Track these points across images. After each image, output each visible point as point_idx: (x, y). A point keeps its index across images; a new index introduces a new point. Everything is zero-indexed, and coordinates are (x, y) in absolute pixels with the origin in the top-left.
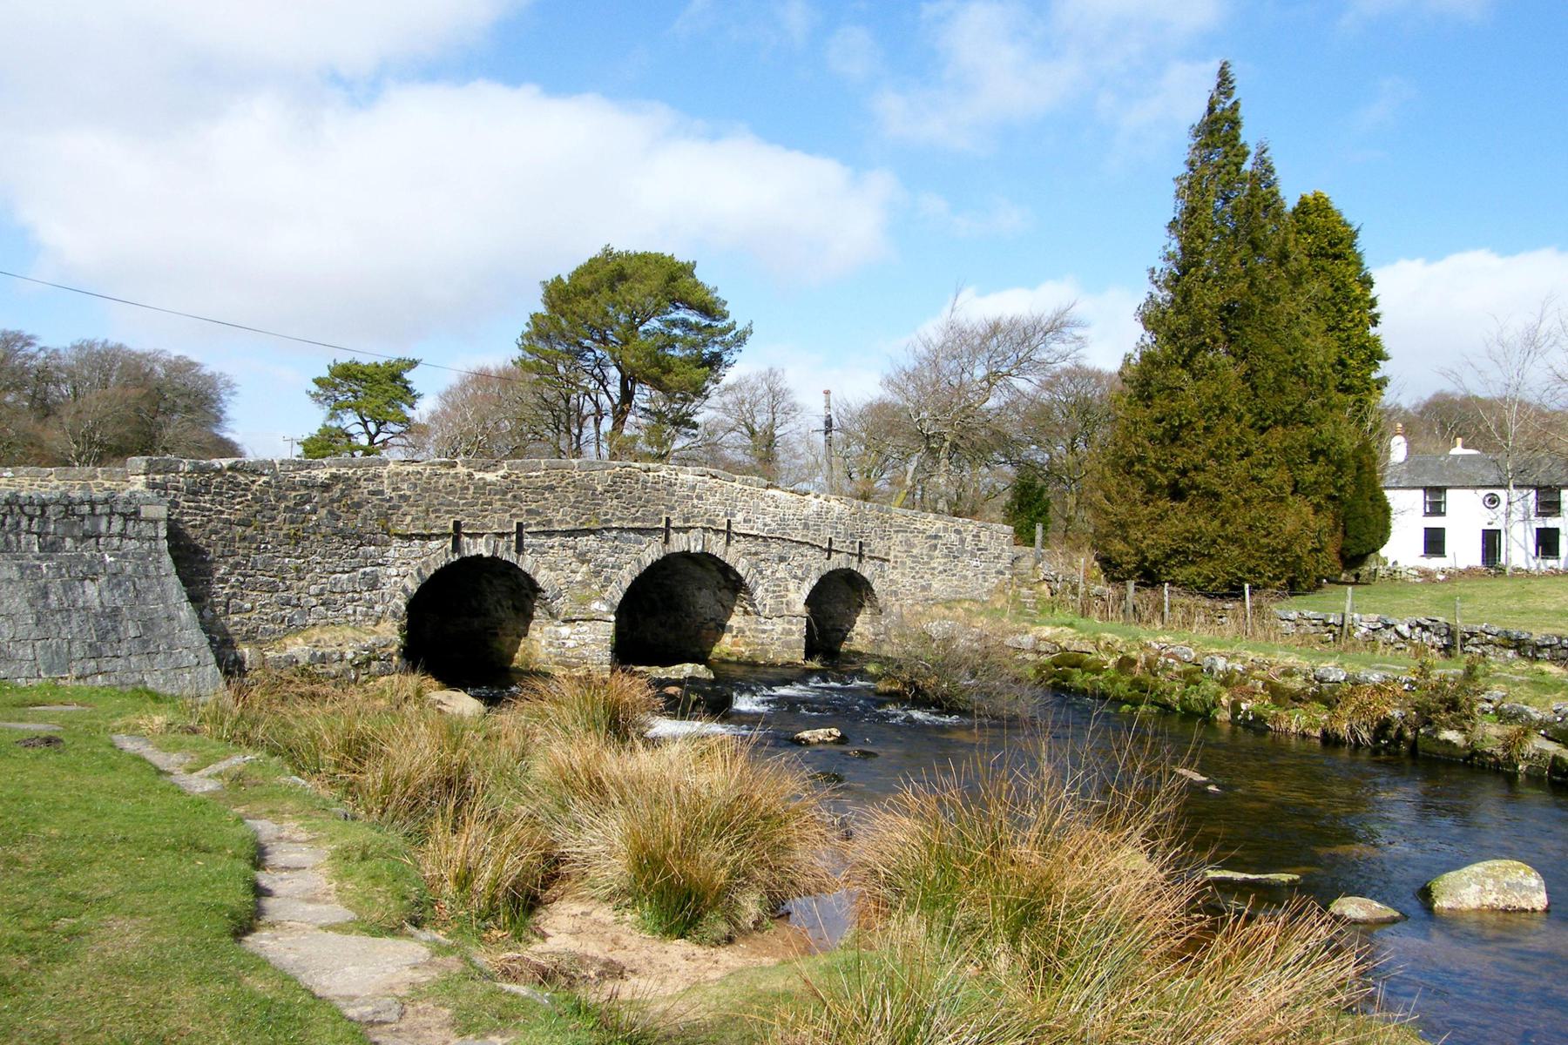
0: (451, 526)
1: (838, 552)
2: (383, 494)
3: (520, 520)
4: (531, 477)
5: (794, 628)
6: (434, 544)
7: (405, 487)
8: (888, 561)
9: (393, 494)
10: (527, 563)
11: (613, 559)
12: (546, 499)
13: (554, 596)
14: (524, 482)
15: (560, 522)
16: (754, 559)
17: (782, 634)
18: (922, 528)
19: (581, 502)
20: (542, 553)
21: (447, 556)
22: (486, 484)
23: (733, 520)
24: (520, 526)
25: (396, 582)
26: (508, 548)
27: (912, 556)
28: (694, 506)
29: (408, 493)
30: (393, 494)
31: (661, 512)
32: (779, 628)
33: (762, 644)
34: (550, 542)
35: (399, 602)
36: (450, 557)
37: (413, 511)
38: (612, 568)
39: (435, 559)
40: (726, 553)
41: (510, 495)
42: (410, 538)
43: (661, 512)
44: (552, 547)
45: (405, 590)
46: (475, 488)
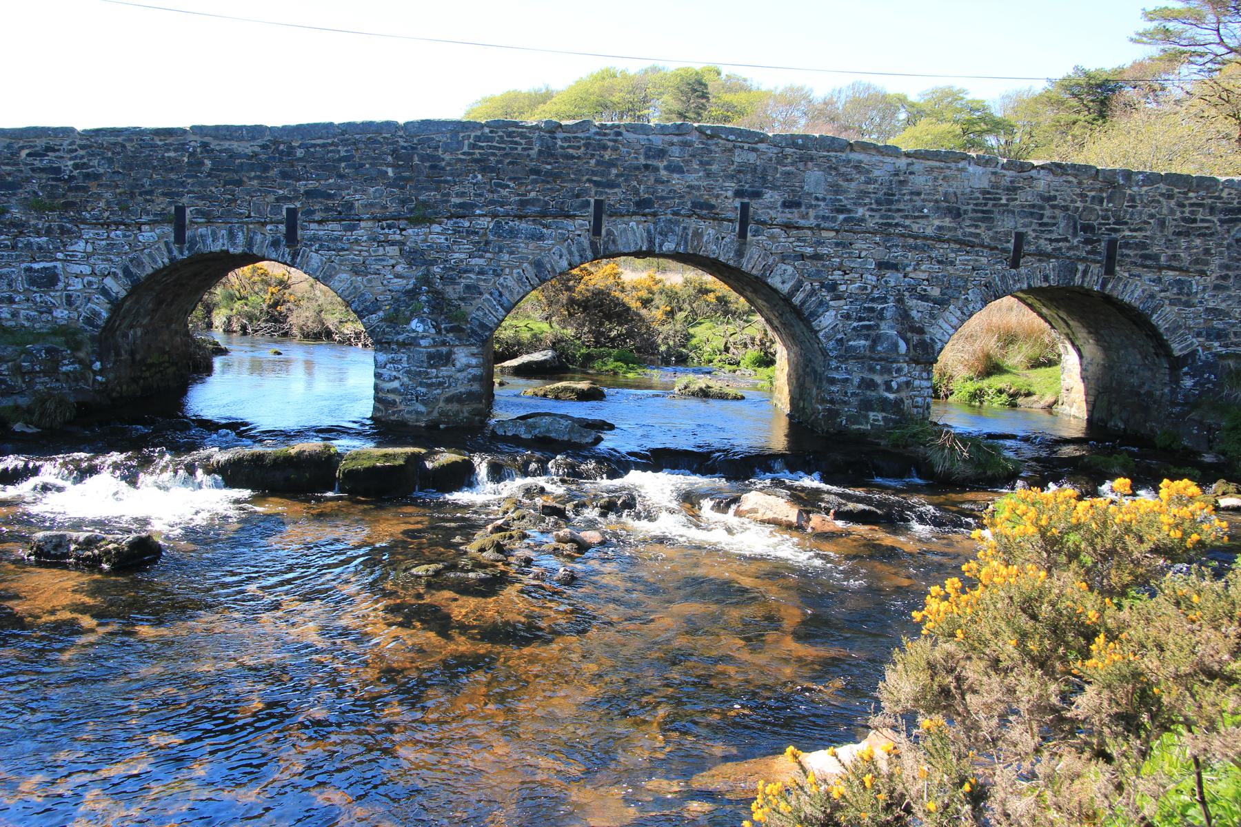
1: (1042, 255)
5: (878, 379)
7: (95, 162)
8: (1202, 273)
9: (76, 173)
11: (481, 261)
16: (810, 266)
17: (859, 387)
21: (170, 251)
22: (233, 155)
23: (754, 205)
24: (292, 213)
28: (659, 181)
30: (76, 173)
31: (585, 192)
32: (856, 381)
33: (832, 401)
35: (97, 308)
36: (176, 253)
37: (108, 195)
38: (481, 272)
39: (150, 255)
40: (740, 254)
41: (273, 173)
42: (107, 225)
43: (585, 192)
45: (105, 292)
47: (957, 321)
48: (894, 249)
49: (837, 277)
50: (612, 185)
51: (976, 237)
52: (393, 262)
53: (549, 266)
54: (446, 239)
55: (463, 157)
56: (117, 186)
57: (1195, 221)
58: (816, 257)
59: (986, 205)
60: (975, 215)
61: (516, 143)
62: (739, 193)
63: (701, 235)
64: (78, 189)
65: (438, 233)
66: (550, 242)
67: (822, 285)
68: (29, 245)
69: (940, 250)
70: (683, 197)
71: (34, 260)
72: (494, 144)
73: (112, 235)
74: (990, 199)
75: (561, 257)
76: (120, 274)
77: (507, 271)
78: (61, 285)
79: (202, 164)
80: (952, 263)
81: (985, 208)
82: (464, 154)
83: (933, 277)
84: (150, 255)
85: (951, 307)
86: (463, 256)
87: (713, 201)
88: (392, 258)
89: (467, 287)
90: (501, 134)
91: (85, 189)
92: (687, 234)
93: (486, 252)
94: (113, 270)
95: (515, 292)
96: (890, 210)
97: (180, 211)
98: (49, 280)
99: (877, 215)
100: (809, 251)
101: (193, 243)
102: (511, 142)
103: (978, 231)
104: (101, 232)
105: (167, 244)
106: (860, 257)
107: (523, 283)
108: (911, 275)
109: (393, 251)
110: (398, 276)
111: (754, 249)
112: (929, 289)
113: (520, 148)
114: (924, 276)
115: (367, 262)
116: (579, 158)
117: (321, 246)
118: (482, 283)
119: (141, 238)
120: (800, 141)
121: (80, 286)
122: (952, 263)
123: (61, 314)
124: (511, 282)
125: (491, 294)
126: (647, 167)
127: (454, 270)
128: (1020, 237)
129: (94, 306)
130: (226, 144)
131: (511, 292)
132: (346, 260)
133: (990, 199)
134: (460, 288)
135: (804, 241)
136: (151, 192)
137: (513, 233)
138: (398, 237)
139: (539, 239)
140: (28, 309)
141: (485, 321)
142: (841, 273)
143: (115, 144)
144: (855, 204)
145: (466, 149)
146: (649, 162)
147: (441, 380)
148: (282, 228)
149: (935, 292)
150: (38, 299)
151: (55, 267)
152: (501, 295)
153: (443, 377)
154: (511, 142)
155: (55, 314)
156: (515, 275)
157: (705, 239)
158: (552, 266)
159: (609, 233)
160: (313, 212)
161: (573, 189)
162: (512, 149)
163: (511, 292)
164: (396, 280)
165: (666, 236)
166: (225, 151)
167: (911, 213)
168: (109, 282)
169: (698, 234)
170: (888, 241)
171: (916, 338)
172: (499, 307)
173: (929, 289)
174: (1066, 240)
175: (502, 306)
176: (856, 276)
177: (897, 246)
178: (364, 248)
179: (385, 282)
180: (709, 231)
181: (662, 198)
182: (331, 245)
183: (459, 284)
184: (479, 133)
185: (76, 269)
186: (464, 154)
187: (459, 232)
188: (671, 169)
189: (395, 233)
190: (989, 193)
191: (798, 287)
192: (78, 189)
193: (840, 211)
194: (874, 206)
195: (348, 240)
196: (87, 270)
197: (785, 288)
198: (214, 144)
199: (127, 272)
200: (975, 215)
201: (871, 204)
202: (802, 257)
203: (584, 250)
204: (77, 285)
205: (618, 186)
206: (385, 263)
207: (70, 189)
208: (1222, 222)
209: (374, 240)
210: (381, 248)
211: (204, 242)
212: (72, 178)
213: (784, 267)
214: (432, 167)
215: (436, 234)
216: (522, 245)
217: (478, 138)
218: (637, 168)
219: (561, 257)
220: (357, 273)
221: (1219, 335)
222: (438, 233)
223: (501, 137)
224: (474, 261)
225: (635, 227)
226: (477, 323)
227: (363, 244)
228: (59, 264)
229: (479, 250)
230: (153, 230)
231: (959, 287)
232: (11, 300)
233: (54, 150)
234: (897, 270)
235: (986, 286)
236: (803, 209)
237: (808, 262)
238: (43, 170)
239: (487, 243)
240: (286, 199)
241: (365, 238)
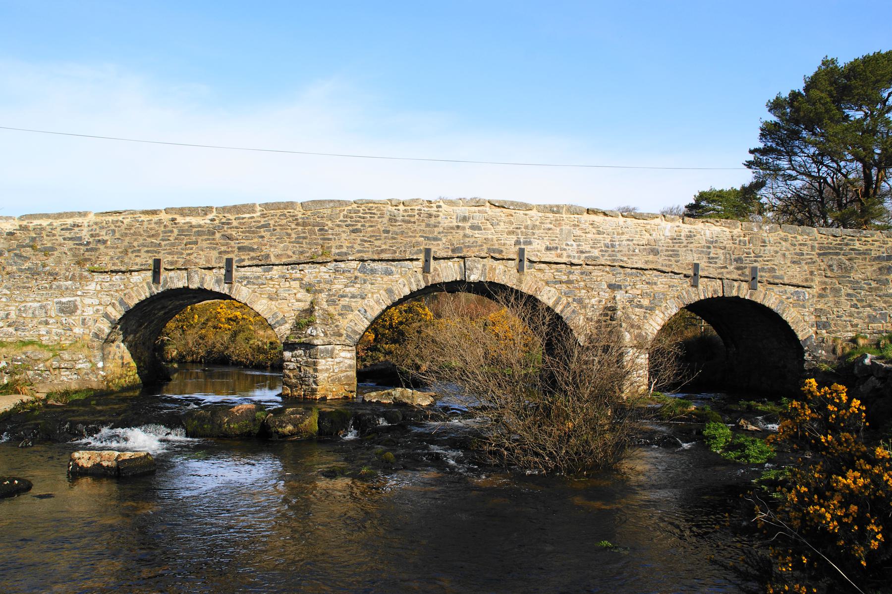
0: (151, 262)
2: (81, 240)
3: (229, 256)
4: (243, 218)
6: (136, 278)
10: (242, 293)
12: (263, 237)
13: (277, 322)
14: (235, 223)
15: (278, 256)
18: (863, 248)
19: (304, 238)
20: (259, 285)
21: (150, 288)
23: (527, 248)
25: (98, 310)
26: (218, 281)
27: (850, 282)
28: (465, 236)
29: (105, 238)
30: (91, 240)
34: (269, 275)
35: (102, 327)
36: (154, 289)
38: (353, 297)
44: (271, 279)
45: (106, 316)
46: (179, 231)
47: (661, 321)
48: (618, 276)
49: (583, 294)
50: (436, 239)
51: (669, 267)
52: (295, 291)
53: (397, 292)
54: (330, 276)
55: (340, 223)
56: (117, 247)
57: (803, 254)
58: (569, 282)
59: (674, 246)
60: (667, 253)
61: (374, 214)
62: (517, 243)
63: (495, 269)
64: (92, 250)
65: (325, 272)
66: (397, 276)
67: (574, 300)
68: (59, 287)
69: (649, 276)
70: (482, 246)
71: (62, 295)
72: (360, 214)
73: (114, 279)
74: (677, 243)
75: (404, 285)
76: (117, 304)
77: (370, 295)
78: (79, 312)
79: (172, 232)
80: (655, 284)
81: (673, 249)
82: (340, 221)
83: (644, 293)
84: (137, 291)
85: (657, 312)
86: (341, 287)
87: (502, 248)
88: (294, 288)
89: (344, 306)
90: (364, 208)
91: (95, 250)
92: (485, 269)
93: (356, 283)
94: (113, 301)
95: (375, 309)
96: (614, 251)
97: (157, 263)
98: (69, 310)
99: (607, 254)
100: (564, 278)
101: (166, 282)
102: (371, 213)
103: (670, 263)
104: (106, 277)
105: (148, 283)
106: (597, 281)
107: (380, 303)
108: (630, 292)
109: (296, 284)
110: (298, 300)
111: (528, 278)
112: (642, 300)
113: (376, 216)
114: (639, 292)
115: (278, 292)
116: (414, 223)
117: (249, 282)
118: (353, 304)
119: (131, 280)
120: (555, 209)
121: (91, 313)
122: (655, 284)
123: (78, 330)
124: (372, 303)
125: (359, 311)
126: (458, 227)
127: (335, 296)
128: (696, 267)
129: (100, 325)
130: (188, 219)
131: (372, 308)
132: (265, 291)
133: (677, 243)
134: (339, 308)
135: (561, 271)
136: (139, 251)
137: (373, 271)
138: (298, 275)
139: (390, 274)
140: (57, 328)
141: (356, 328)
142: (585, 291)
143: (117, 221)
144: (591, 247)
145: (342, 218)
146: (460, 224)
147: (328, 367)
148: (223, 271)
149: (646, 302)
150: (64, 322)
151: (76, 300)
152: (366, 311)
153: (329, 365)
154: (371, 213)
155: (74, 331)
156: (375, 298)
157: (497, 271)
158: (399, 292)
159: (435, 270)
160: (243, 260)
161: (411, 242)
162: (371, 217)
163: (372, 308)
164: (297, 303)
165: (472, 270)
166: (188, 223)
167: (627, 253)
168: (110, 309)
169: (493, 269)
170: (614, 270)
171: (636, 331)
172: (365, 319)
173: (642, 300)
174: (726, 267)
175: (366, 318)
176: (596, 293)
177: (620, 273)
178: (277, 283)
179: (290, 305)
180: (499, 266)
181: (469, 247)
182: (255, 281)
183: (337, 305)
184: (350, 208)
185: (87, 301)
186: (340, 221)
187: (338, 271)
188: (473, 227)
189: (296, 273)
190: (675, 239)
191: (557, 303)
192: (92, 250)
193: (582, 252)
194: (603, 249)
195: (266, 278)
196: (96, 302)
197: (550, 303)
198: (180, 220)
199: (122, 302)
200: (667, 253)
201: (602, 247)
202: (561, 282)
203: (419, 281)
204: (89, 312)
205: (440, 240)
206: (290, 292)
207: (87, 250)
208: (819, 255)
209: (283, 277)
210: (287, 283)
211: (173, 282)
212: (88, 243)
213: (549, 288)
214: (320, 230)
215: (323, 272)
216: (379, 279)
217: (350, 211)
218: (452, 228)
219: (404, 285)
220: (271, 299)
221: (825, 325)
222: (325, 272)
223: (363, 210)
224: (348, 290)
225: (452, 266)
226: (351, 330)
227: (277, 280)
228: (78, 298)
229: (351, 282)
230: (139, 275)
231: (661, 299)
232: (47, 323)
233: (78, 226)
234: (621, 288)
235: (678, 298)
236: (559, 251)
237: (564, 286)
238: (71, 239)
239: (356, 278)
240: (226, 252)
241: (277, 276)
